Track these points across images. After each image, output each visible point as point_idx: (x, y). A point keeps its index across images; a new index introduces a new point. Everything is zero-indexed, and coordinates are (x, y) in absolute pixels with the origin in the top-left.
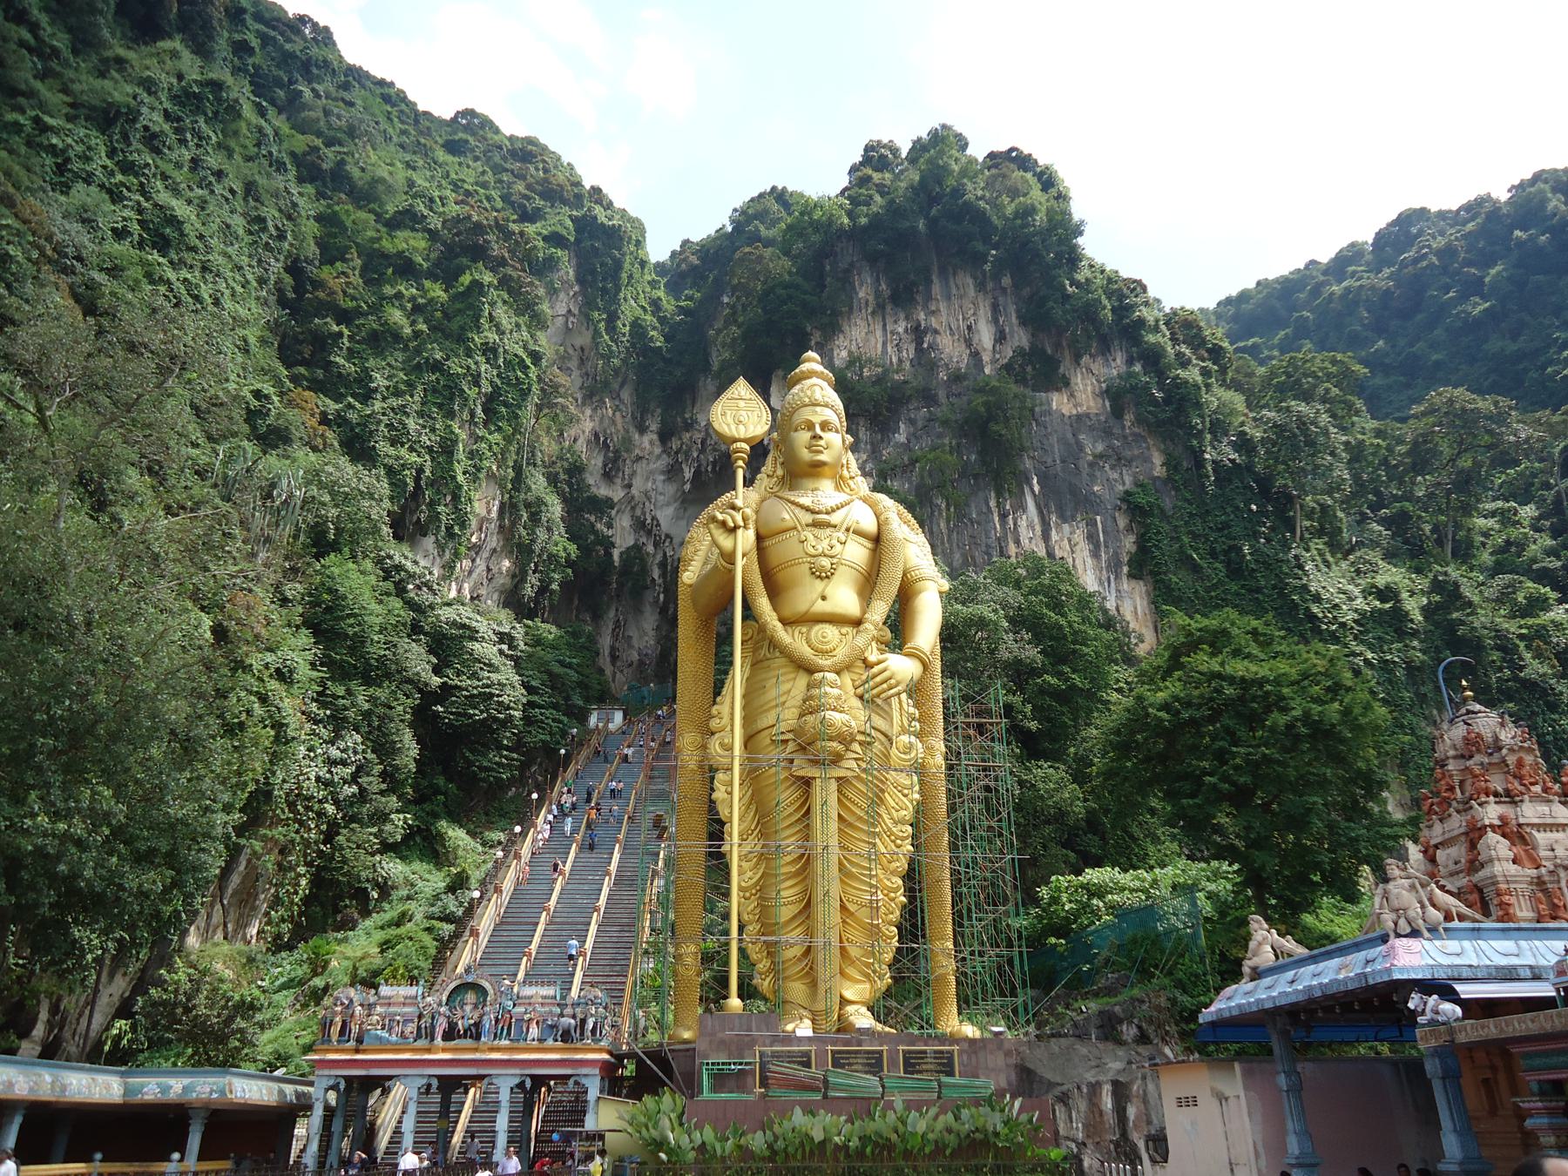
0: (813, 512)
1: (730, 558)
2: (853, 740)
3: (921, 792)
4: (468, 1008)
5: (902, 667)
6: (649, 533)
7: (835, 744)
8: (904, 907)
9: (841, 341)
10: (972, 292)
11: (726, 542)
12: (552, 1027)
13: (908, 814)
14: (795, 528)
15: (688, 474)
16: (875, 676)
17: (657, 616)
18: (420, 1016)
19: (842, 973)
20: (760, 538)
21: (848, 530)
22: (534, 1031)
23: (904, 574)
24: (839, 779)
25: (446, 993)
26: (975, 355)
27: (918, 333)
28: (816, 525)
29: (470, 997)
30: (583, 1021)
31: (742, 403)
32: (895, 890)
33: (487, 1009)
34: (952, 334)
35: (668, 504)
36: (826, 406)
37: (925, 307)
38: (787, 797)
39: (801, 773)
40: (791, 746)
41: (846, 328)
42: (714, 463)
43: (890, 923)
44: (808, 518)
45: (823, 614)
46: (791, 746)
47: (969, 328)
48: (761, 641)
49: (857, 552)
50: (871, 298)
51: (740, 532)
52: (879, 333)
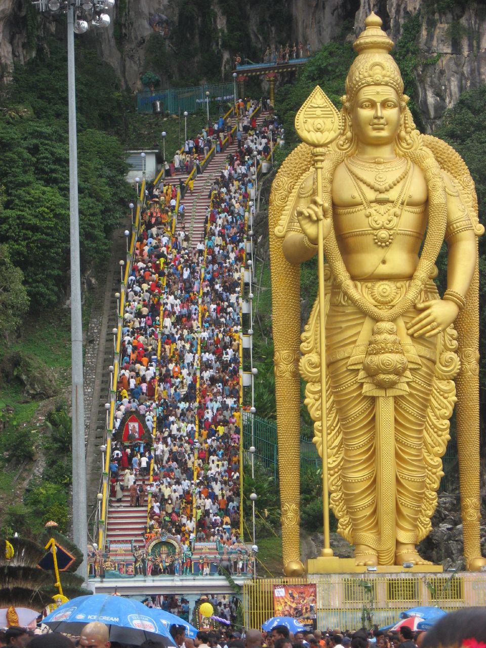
0: (376, 190)
1: (315, 241)
2: (404, 369)
3: (457, 396)
4: (164, 556)
5: (442, 310)
8: (444, 482)
11: (311, 229)
12: (217, 566)
13: (448, 412)
16: (421, 320)
18: (136, 562)
19: (397, 525)
20: (334, 205)
21: (402, 204)
22: (207, 570)
23: (449, 224)
24: (395, 397)
25: (150, 548)
29: (164, 549)
30: (236, 563)
31: (319, 112)
32: (436, 467)
33: (177, 557)
36: (386, 84)
38: (357, 410)
39: (368, 394)
40: (362, 374)
43: (433, 490)
44: (371, 195)
45: (383, 275)
46: (362, 374)
48: (335, 287)
49: (408, 220)
51: (321, 223)
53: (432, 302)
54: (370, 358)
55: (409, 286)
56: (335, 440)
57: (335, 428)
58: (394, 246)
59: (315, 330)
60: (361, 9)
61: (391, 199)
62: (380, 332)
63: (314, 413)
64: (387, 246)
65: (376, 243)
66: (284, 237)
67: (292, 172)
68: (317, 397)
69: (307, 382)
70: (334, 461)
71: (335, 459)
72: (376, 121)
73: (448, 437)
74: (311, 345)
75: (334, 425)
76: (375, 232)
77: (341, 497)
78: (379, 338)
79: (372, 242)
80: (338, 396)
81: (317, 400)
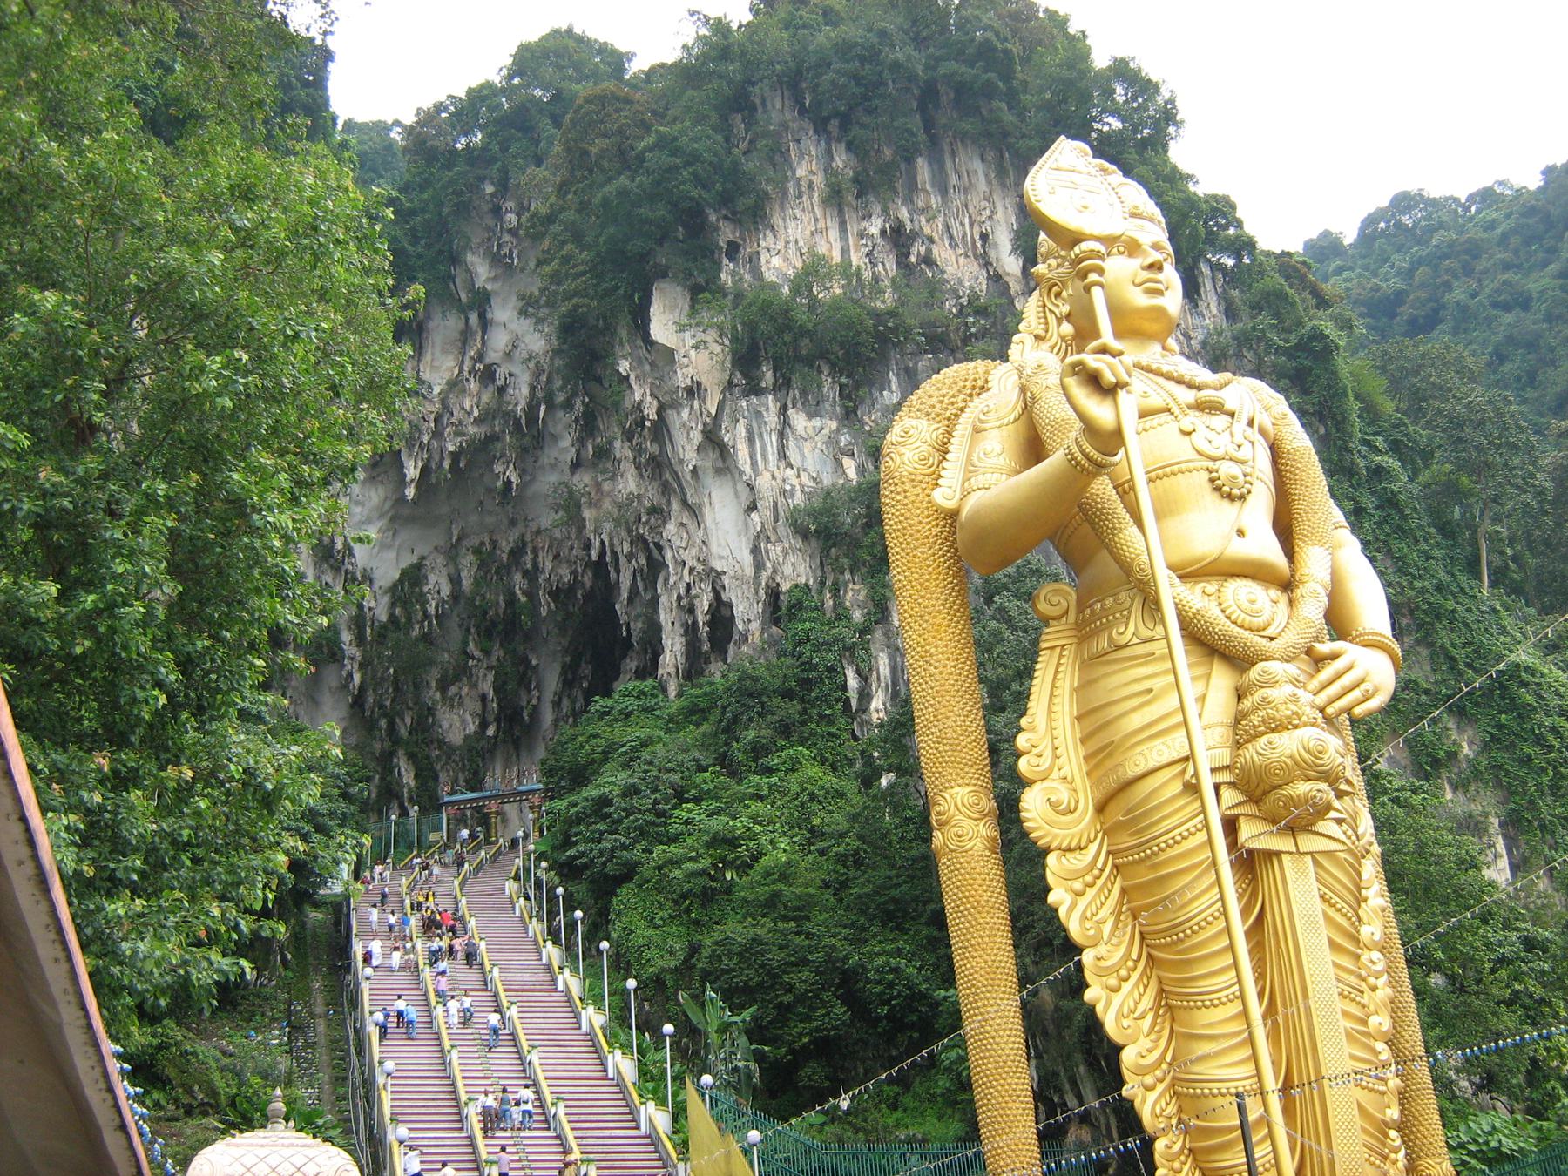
0: (1190, 386)
6: (337, 570)
7: (1324, 786)
9: (767, 241)
10: (982, 185)
14: (1169, 410)
15: (412, 471)
17: (343, 711)
21: (1251, 423)
26: (996, 278)
27: (899, 238)
28: (1200, 407)
34: (953, 244)
35: (368, 521)
37: (909, 200)
41: (777, 220)
42: (455, 456)
47: (984, 237)
50: (819, 180)
51: (1121, 394)
52: (834, 234)
53: (1339, 645)
54: (1264, 739)
55: (1291, 602)
56: (1141, 995)
57: (1138, 960)
58: (1250, 498)
59: (1048, 730)
60: (668, 653)
61: (1229, 406)
62: (1271, 683)
63: (1075, 930)
64: (1242, 497)
65: (1218, 489)
66: (953, 515)
67: (937, 410)
68: (1078, 886)
69: (1046, 852)
70: (1150, 1051)
71: (1150, 1045)
72: (1146, 275)
73: (1389, 991)
74: (1046, 762)
75: (1134, 956)
76: (1211, 464)
77: (1184, 1146)
78: (1274, 694)
79: (1208, 487)
80: (1155, 867)
81: (1080, 894)
